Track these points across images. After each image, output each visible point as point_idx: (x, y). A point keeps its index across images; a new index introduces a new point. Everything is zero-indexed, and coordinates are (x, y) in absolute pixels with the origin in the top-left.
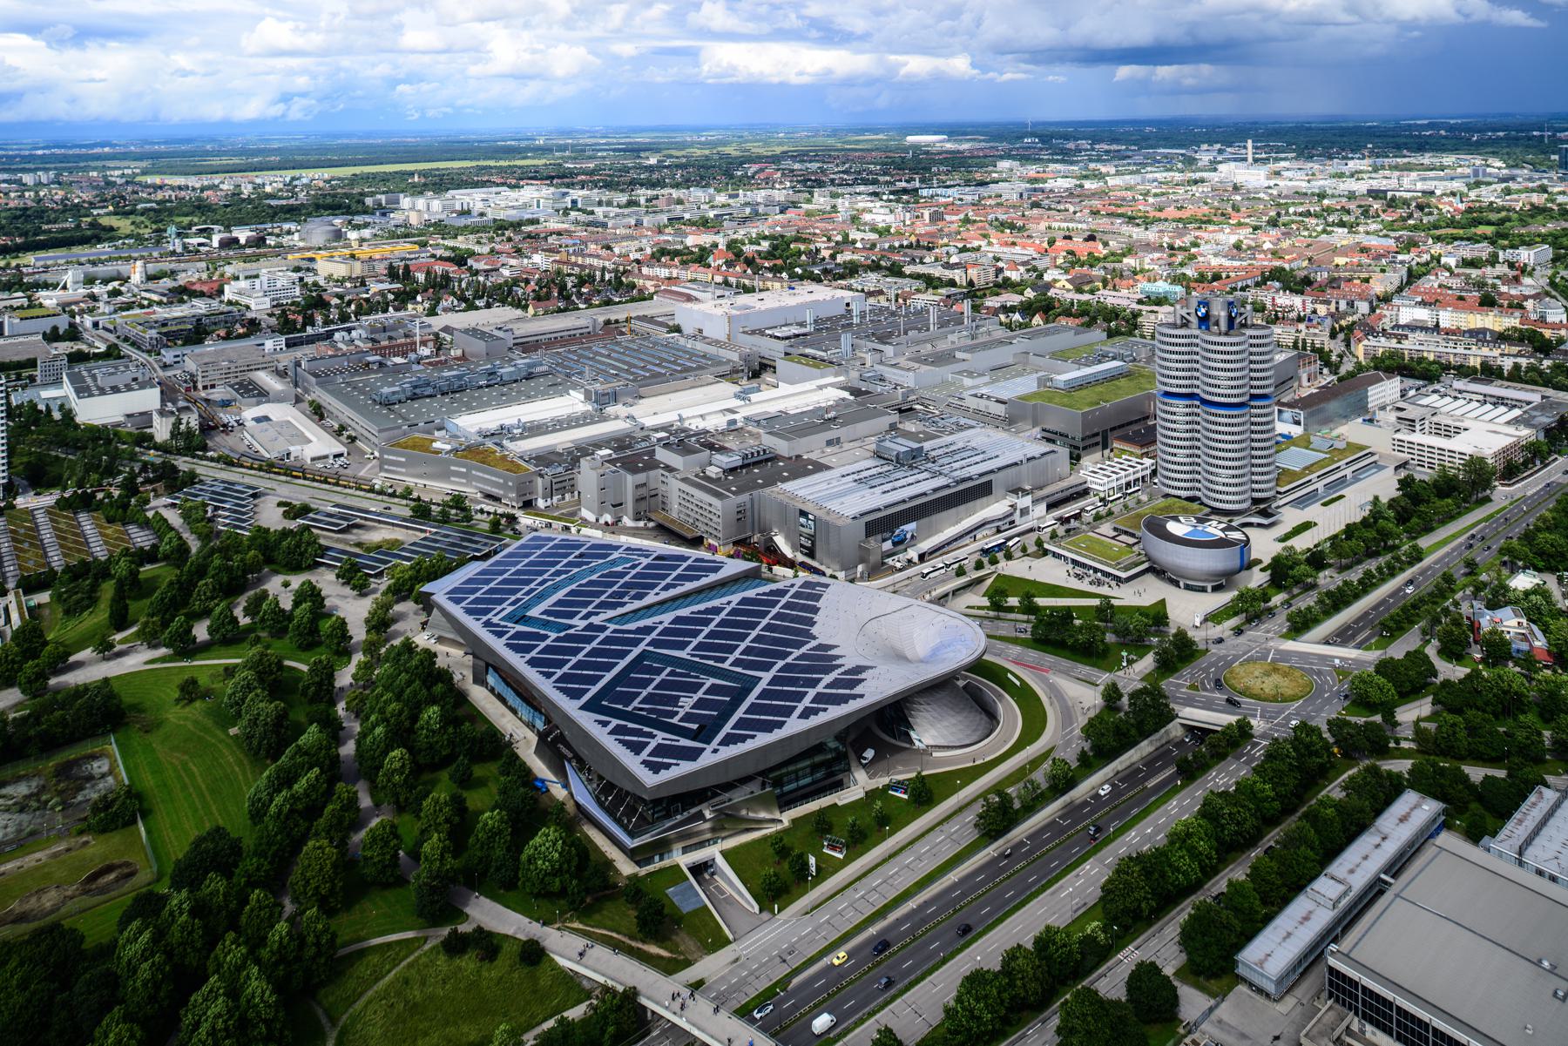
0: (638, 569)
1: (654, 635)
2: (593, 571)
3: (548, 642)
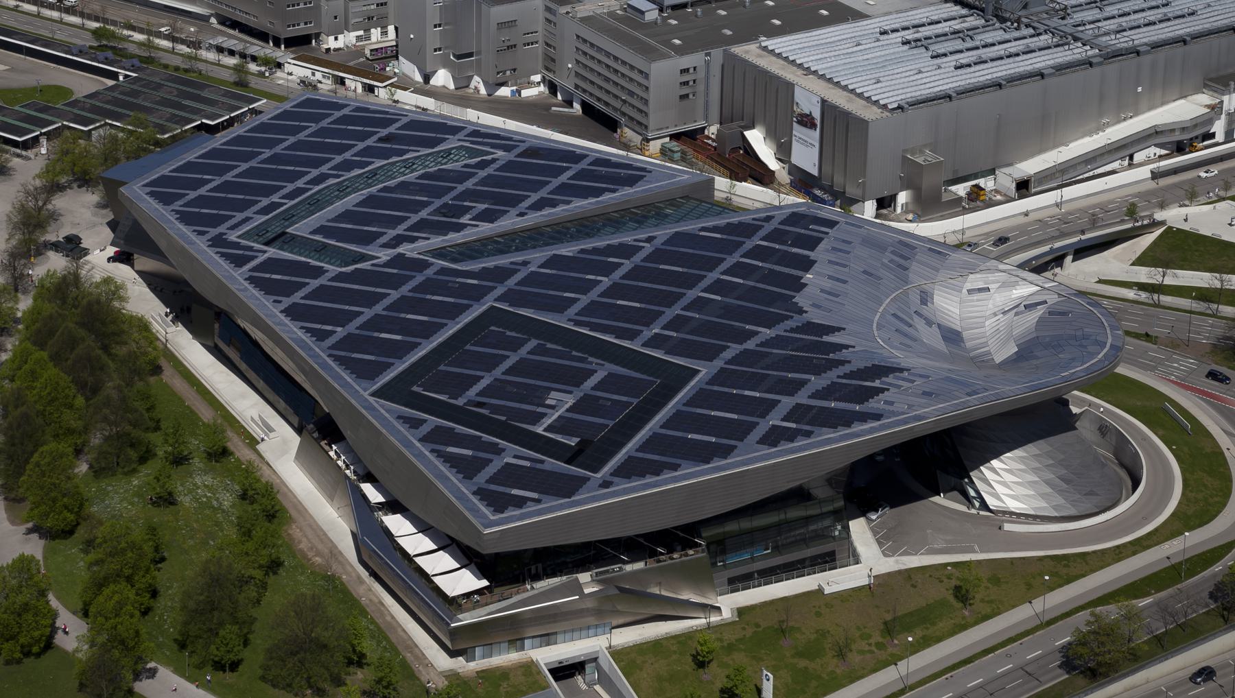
0: (490, 170)
1: (511, 282)
2: (409, 165)
3: (322, 281)
